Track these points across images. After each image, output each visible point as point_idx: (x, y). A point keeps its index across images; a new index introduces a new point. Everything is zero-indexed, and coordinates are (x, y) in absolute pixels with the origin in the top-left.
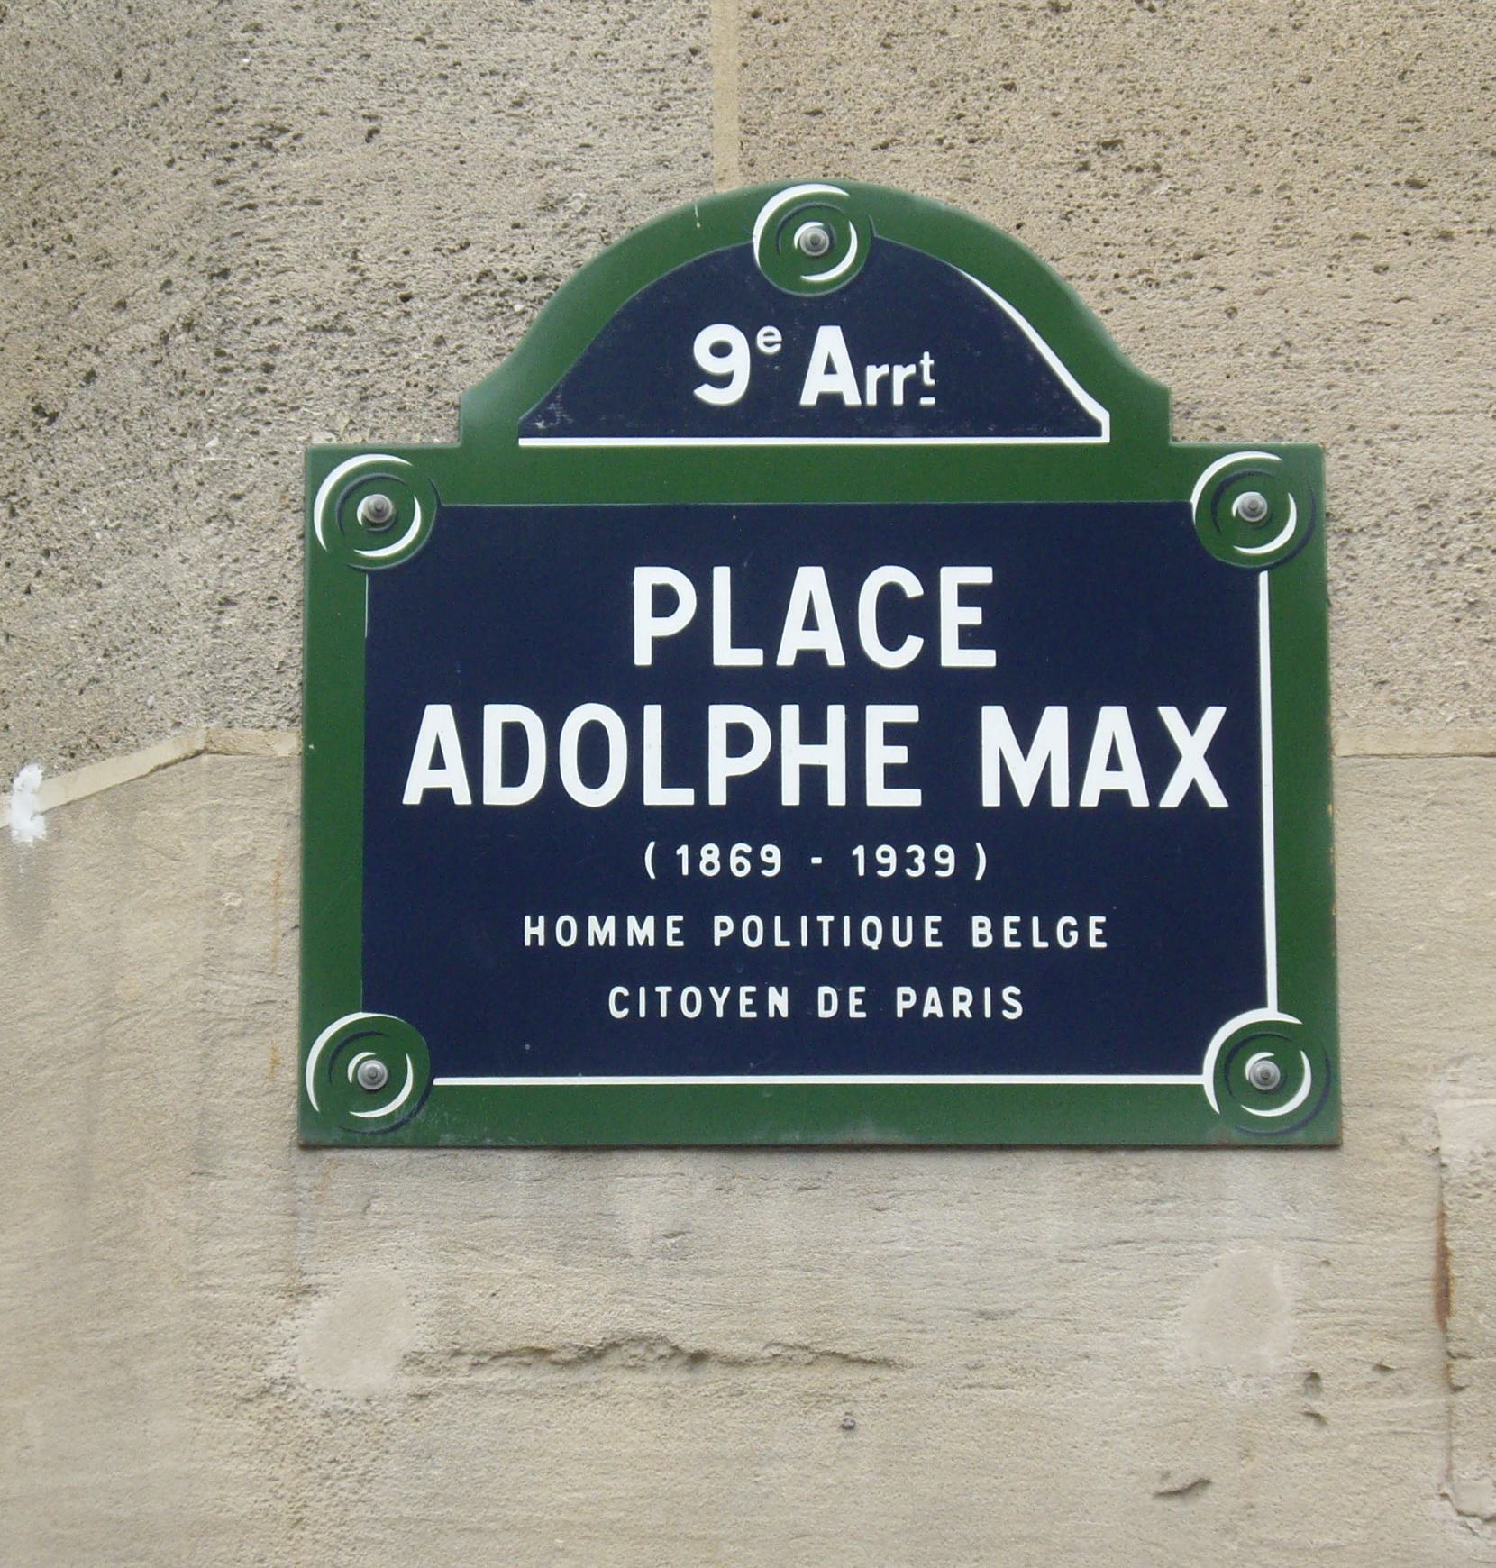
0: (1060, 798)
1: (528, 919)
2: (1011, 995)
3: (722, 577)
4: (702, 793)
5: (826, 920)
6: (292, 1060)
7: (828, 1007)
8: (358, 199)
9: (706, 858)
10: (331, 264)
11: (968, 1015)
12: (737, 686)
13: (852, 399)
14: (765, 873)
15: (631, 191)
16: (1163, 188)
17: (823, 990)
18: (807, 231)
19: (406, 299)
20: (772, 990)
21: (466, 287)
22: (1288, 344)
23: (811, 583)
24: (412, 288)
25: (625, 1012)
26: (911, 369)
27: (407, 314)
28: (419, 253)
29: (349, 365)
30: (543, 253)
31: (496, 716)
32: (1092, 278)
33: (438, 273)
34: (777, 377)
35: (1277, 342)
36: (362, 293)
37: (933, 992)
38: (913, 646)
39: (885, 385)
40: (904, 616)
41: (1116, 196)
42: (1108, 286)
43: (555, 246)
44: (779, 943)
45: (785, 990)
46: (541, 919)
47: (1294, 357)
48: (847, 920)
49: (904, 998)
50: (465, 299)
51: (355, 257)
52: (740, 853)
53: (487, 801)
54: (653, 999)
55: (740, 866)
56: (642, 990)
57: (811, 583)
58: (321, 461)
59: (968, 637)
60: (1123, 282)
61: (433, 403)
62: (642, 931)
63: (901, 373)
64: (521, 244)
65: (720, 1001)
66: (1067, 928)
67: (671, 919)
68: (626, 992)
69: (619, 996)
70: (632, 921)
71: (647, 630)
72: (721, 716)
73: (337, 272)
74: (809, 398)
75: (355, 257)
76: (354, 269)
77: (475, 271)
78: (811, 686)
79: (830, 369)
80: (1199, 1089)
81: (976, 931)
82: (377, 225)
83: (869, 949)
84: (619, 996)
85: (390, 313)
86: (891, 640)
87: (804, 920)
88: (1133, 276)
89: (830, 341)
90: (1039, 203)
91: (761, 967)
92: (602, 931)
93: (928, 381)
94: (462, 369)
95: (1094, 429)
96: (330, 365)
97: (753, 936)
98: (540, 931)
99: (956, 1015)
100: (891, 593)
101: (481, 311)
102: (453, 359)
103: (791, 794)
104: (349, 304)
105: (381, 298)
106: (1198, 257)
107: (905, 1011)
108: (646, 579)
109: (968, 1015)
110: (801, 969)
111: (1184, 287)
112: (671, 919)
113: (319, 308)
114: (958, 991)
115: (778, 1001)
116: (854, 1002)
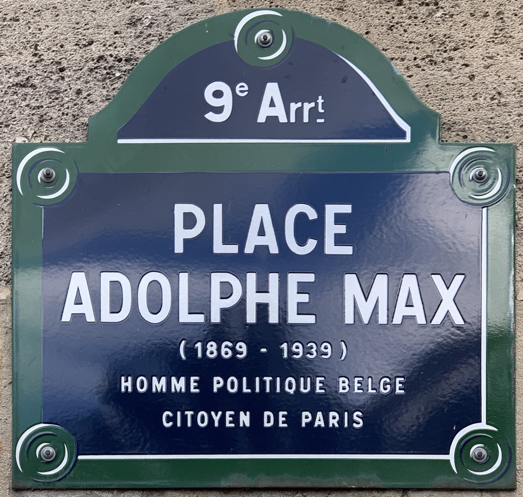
0: (383, 319)
1: (123, 378)
2: (358, 416)
3: (218, 209)
4: (208, 318)
5: (268, 379)
6: (9, 448)
7: (269, 422)
8: (37, 18)
9: (209, 349)
10: (24, 51)
11: (337, 425)
12: (225, 263)
13: (283, 119)
14: (238, 356)
15: (174, 14)
16: (439, 14)
17: (266, 413)
18: (260, 34)
19: (62, 70)
20: (242, 413)
21: (91, 64)
22: (499, 93)
23: (262, 212)
24: (64, 64)
25: (171, 424)
26: (313, 105)
27: (63, 78)
28: (68, 47)
29: (34, 104)
30: (130, 47)
31: (107, 278)
32: (403, 60)
33: (78, 57)
34: (246, 107)
35: (494, 92)
36: (40, 67)
37: (319, 415)
38: (311, 244)
39: (299, 112)
40: (307, 229)
41: (416, 18)
42: (411, 63)
43: (135, 43)
44: (245, 390)
45: (248, 413)
46: (130, 378)
47: (503, 100)
48: (278, 379)
49: (306, 417)
50: (91, 70)
51: (36, 49)
52: (226, 347)
53: (103, 320)
54: (184, 418)
55: (226, 353)
56: (179, 413)
57: (262, 212)
58: (19, 151)
59: (339, 240)
60: (418, 61)
61: (75, 123)
62: (179, 385)
63: (307, 106)
64: (119, 42)
65: (216, 419)
66: (385, 384)
67: (192, 379)
68: (171, 414)
69: (168, 416)
70: (174, 379)
71: (181, 235)
72: (217, 279)
73: (28, 56)
74: (261, 119)
75: (36, 49)
76: (35, 55)
77: (96, 56)
78: (261, 263)
79: (273, 105)
80: (448, 461)
81: (341, 385)
82: (46, 32)
83: (288, 393)
84: (168, 416)
85: (54, 77)
86: (301, 242)
87: (257, 379)
88: (423, 59)
89: (272, 90)
90: (377, 22)
91: (239, 402)
92: (159, 385)
93: (321, 110)
94: (90, 106)
95: (402, 134)
96: (24, 103)
97: (232, 387)
98: (129, 384)
99: (331, 425)
100: (301, 217)
101: (99, 76)
102: (85, 101)
103: (251, 318)
104: (33, 72)
105: (49, 69)
106: (455, 49)
107: (306, 424)
108: (180, 210)
109: (337, 425)
110: (256, 404)
111: (450, 64)
112: (192, 379)
113: (18, 74)
114: (332, 414)
115: (245, 419)
116: (281, 419)
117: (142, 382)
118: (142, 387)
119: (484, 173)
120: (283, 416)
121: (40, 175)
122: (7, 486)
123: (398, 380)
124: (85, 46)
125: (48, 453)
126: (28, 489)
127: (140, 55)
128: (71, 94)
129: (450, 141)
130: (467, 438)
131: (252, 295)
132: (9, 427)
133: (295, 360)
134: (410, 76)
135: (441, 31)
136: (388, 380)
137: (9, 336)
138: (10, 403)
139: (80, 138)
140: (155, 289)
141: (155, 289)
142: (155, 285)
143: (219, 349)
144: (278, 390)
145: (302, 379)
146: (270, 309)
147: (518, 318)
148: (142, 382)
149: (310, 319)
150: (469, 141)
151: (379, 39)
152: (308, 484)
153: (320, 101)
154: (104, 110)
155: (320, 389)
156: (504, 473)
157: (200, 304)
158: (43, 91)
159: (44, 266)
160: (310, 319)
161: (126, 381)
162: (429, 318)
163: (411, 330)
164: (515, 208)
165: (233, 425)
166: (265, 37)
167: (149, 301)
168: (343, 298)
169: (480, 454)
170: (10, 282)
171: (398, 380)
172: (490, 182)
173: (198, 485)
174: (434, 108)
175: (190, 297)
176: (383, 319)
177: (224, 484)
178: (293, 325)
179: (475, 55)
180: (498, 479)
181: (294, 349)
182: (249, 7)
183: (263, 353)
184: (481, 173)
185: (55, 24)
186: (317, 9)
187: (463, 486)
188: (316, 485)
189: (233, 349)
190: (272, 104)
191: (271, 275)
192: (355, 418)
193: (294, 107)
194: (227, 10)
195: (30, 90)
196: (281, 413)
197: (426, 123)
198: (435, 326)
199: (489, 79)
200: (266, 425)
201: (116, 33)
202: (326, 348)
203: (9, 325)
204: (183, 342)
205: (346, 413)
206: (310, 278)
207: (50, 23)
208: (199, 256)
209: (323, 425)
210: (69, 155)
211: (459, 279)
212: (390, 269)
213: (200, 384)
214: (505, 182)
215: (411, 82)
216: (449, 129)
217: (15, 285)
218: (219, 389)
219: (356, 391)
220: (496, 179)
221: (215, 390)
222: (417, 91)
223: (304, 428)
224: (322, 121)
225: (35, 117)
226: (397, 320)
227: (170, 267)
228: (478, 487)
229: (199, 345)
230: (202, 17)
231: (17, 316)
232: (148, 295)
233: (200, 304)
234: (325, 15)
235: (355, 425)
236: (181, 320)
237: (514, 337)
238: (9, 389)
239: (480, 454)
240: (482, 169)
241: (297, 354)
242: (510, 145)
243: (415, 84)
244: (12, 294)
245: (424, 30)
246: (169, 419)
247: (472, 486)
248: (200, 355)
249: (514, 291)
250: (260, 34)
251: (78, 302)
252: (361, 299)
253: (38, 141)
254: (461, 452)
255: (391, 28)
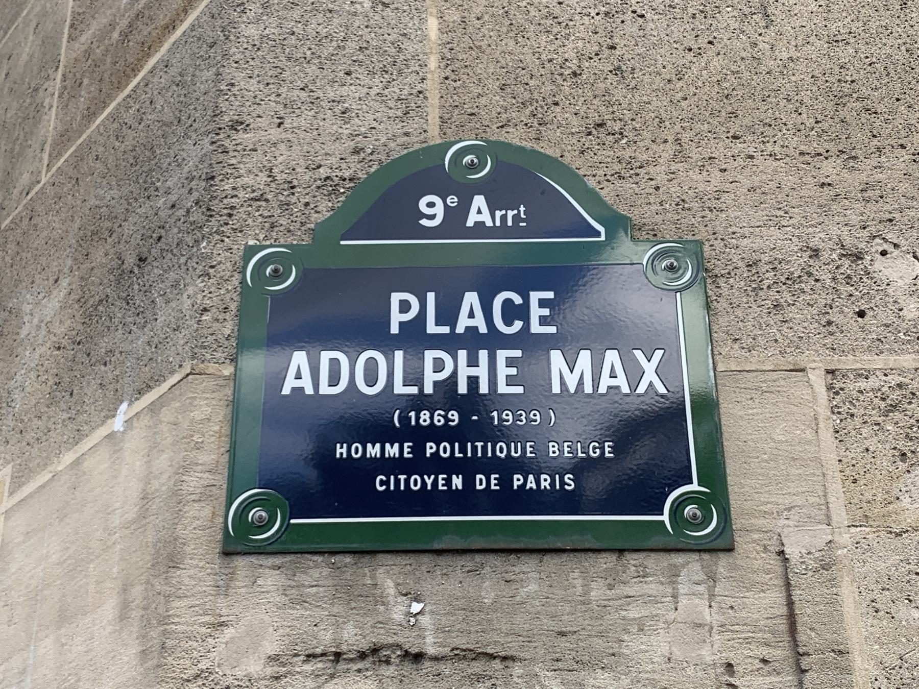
0: (588, 389)
1: (338, 445)
2: (569, 478)
3: (431, 297)
4: (421, 390)
5: (479, 445)
6: (222, 512)
7: (481, 484)
8: (273, 149)
9: (422, 417)
10: (260, 174)
11: (548, 487)
12: (437, 342)
13: (489, 223)
14: (451, 423)
15: (392, 145)
16: (624, 141)
17: (478, 477)
18: (468, 159)
19: (293, 188)
20: (454, 477)
21: (319, 183)
22: (683, 201)
23: (471, 299)
24: (295, 183)
25: (384, 487)
26: (515, 212)
27: (293, 194)
28: (298, 170)
29: (266, 213)
30: (353, 169)
31: (326, 356)
32: (594, 176)
33: (307, 177)
34: (455, 220)
35: (678, 200)
36: (273, 185)
37: (531, 477)
38: (518, 325)
39: (504, 218)
41: (604, 144)
42: (602, 178)
43: (358, 166)
44: (457, 455)
45: (460, 476)
46: (345, 445)
47: (686, 205)
48: (489, 444)
49: (517, 480)
50: (319, 187)
51: (271, 172)
52: (439, 415)
53: (321, 393)
54: (397, 482)
55: (439, 421)
56: (392, 477)
57: (471, 299)
58: (250, 252)
59: (543, 321)
60: (608, 177)
61: (303, 228)
62: (392, 451)
63: (511, 214)
64: (344, 166)
65: (429, 482)
66: (594, 448)
67: (406, 445)
68: (384, 478)
69: (381, 480)
70: (388, 446)
71: (396, 319)
72: (430, 356)
73: (263, 177)
74: (470, 223)
75: (271, 172)
76: (270, 176)
77: (323, 177)
78: (473, 341)
79: (479, 211)
80: (663, 522)
81: (551, 449)
82: (280, 159)
83: (500, 458)
84: (381, 480)
85: (285, 193)
86: (508, 323)
87: (469, 444)
88: (612, 175)
89: (479, 201)
90: (569, 148)
91: (450, 466)
92: (373, 451)
93: (523, 216)
94: (316, 215)
95: (598, 234)
96: (257, 214)
97: (445, 452)
98: (344, 450)
99: (543, 487)
100: (507, 303)
101: (325, 192)
102: (312, 211)
103: (462, 389)
104: (267, 189)
105: (282, 187)
106: (640, 167)
107: (518, 486)
108: (396, 298)
109: (548, 487)
110: (467, 468)
111: (637, 179)
112: (406, 445)
113: (254, 191)
114: (543, 477)
115: (457, 482)
116: (493, 482)
117: (357, 449)
118: (357, 453)
119: (675, 264)
120: (495, 479)
121: (268, 271)
122: (218, 550)
123: (607, 444)
124: (314, 169)
125: (261, 517)
126: (238, 554)
127: (362, 175)
128: (300, 206)
129: (641, 239)
130: (681, 499)
131: (462, 369)
132: (224, 493)
133: (505, 426)
134: (602, 189)
135: (627, 154)
136: (597, 445)
137: (230, 408)
138: (226, 470)
139: (307, 240)
140: (371, 365)
141: (371, 365)
142: (371, 363)
143: (432, 418)
144: (490, 455)
145: (513, 444)
146: (481, 381)
147: (719, 387)
148: (357, 449)
149: (519, 390)
150: (659, 238)
151: (572, 160)
152: (522, 546)
153: (522, 209)
154: (329, 218)
155: (531, 452)
156: (721, 533)
157: (414, 377)
158: (275, 204)
159: (268, 346)
160: (519, 390)
161: (342, 447)
162: (633, 386)
163: (617, 398)
164: (706, 292)
165: (445, 488)
166: (472, 161)
167: (366, 375)
168: (550, 371)
169: (695, 515)
170: (234, 360)
171: (607, 444)
172: (681, 272)
173: (409, 547)
174: (625, 213)
175: (404, 371)
176: (588, 389)
177: (436, 546)
178: (501, 395)
179: (659, 173)
180: (716, 539)
181: (504, 416)
182: (457, 138)
183: (475, 420)
184: (672, 264)
185: (289, 153)
186: (517, 140)
187: (680, 546)
188: (531, 546)
189: (445, 417)
190: (479, 212)
191: (480, 351)
192: (566, 480)
193: (498, 214)
194: (439, 141)
195: (263, 204)
196: (493, 476)
197: (617, 223)
198: (639, 395)
199: (673, 189)
200: (478, 487)
201: (342, 159)
202: (535, 415)
203: (230, 398)
204: (398, 412)
205: (557, 476)
206: (518, 353)
207: (284, 152)
208: (414, 337)
209: (535, 487)
210: (296, 254)
211: (659, 354)
212: (592, 346)
213: (413, 450)
214: (695, 271)
215: (603, 193)
216: (639, 229)
217: (239, 363)
218: (431, 454)
219: (566, 454)
220: (687, 269)
221: (428, 455)
222: (609, 200)
223: (515, 491)
224: (525, 224)
225: (266, 224)
226: (602, 389)
227: (387, 346)
228: (695, 548)
229: (412, 414)
230: (417, 147)
231: (239, 390)
232: (365, 370)
233: (414, 377)
234: (524, 144)
235: (567, 487)
236: (396, 392)
237: (717, 404)
238: (226, 456)
239: (695, 515)
240: (673, 260)
241: (508, 421)
242: (697, 241)
243: (607, 194)
244: (236, 371)
245: (612, 153)
246: (382, 483)
247: (690, 547)
248: (413, 423)
249: (713, 363)
250: (468, 159)
251: (298, 377)
252: (565, 372)
253: (268, 243)
254: (675, 513)
255: (582, 152)
